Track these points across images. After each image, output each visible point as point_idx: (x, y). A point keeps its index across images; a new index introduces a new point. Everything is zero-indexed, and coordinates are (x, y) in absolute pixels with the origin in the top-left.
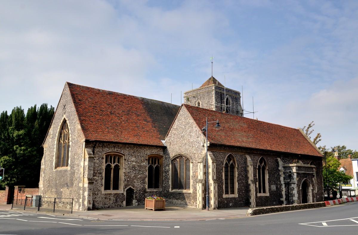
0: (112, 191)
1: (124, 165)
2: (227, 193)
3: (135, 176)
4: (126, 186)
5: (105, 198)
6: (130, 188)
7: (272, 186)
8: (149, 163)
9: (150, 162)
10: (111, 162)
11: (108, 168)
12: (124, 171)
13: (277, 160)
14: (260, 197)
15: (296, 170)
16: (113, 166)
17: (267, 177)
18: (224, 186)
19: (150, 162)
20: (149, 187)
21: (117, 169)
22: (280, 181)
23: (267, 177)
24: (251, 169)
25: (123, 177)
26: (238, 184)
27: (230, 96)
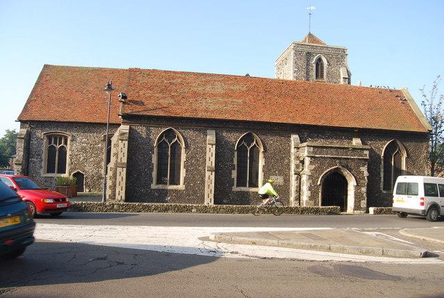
0: (55, 175)
4: (72, 169)
6: (78, 172)
11: (51, 150)
14: (237, 192)
15: (309, 152)
17: (261, 163)
21: (63, 152)
24: (211, 152)
26: (187, 171)
27: (325, 54)
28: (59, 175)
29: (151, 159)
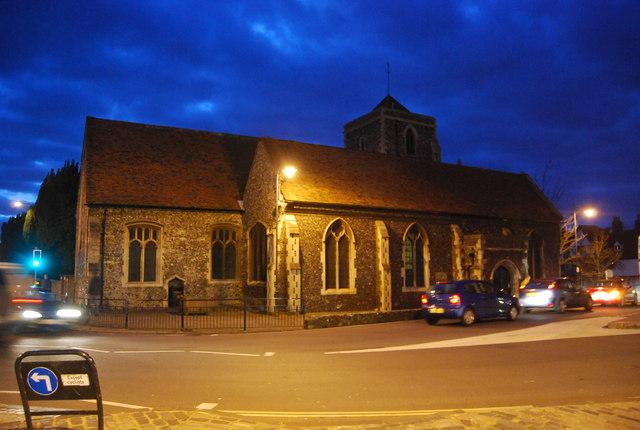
0: (143, 284)
1: (162, 242)
2: (330, 284)
3: (186, 260)
4: (167, 276)
5: (129, 294)
7: (438, 274)
8: (214, 238)
9: (218, 236)
10: (140, 237)
11: (135, 249)
12: (163, 251)
13: (450, 229)
16: (143, 243)
18: (324, 275)
19: (218, 236)
20: (216, 275)
21: (152, 249)
22: (456, 266)
23: (427, 257)
25: (162, 262)
27: (414, 125)
28: (147, 285)
29: (319, 257)
